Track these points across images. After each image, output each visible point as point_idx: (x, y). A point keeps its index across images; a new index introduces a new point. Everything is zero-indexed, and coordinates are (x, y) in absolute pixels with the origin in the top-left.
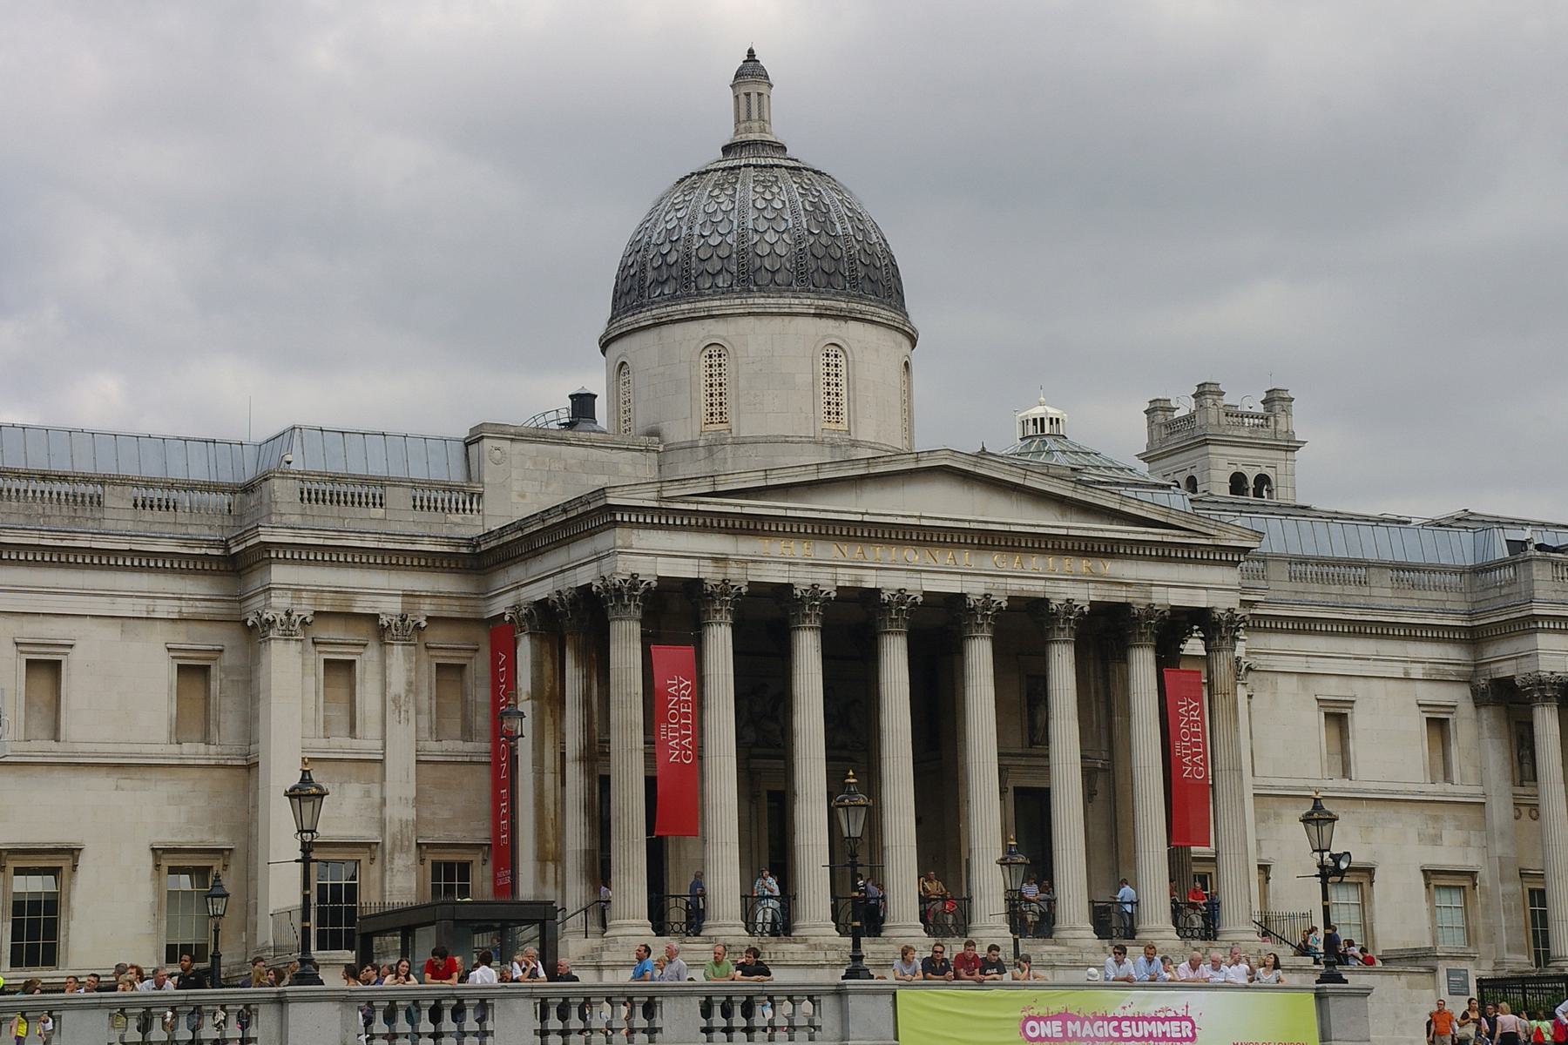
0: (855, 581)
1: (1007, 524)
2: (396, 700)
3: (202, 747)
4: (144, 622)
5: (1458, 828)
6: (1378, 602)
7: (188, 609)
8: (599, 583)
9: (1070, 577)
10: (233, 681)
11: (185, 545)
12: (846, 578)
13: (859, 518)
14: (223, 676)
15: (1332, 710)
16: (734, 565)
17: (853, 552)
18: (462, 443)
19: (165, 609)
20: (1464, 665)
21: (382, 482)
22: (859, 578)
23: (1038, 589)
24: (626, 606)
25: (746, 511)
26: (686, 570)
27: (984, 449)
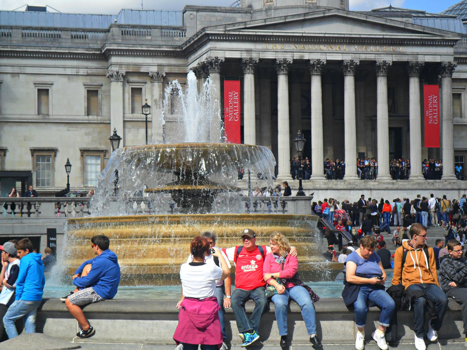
0: (301, 57)
1: (359, 35)
2: (155, 101)
3: (95, 117)
7: (90, 72)
8: (206, 60)
10: (106, 95)
12: (297, 56)
13: (301, 35)
14: (102, 93)
16: (254, 53)
17: (300, 47)
18: (182, 13)
19: (82, 72)
23: (372, 57)
24: (214, 68)
26: (236, 55)
27: (391, 6)
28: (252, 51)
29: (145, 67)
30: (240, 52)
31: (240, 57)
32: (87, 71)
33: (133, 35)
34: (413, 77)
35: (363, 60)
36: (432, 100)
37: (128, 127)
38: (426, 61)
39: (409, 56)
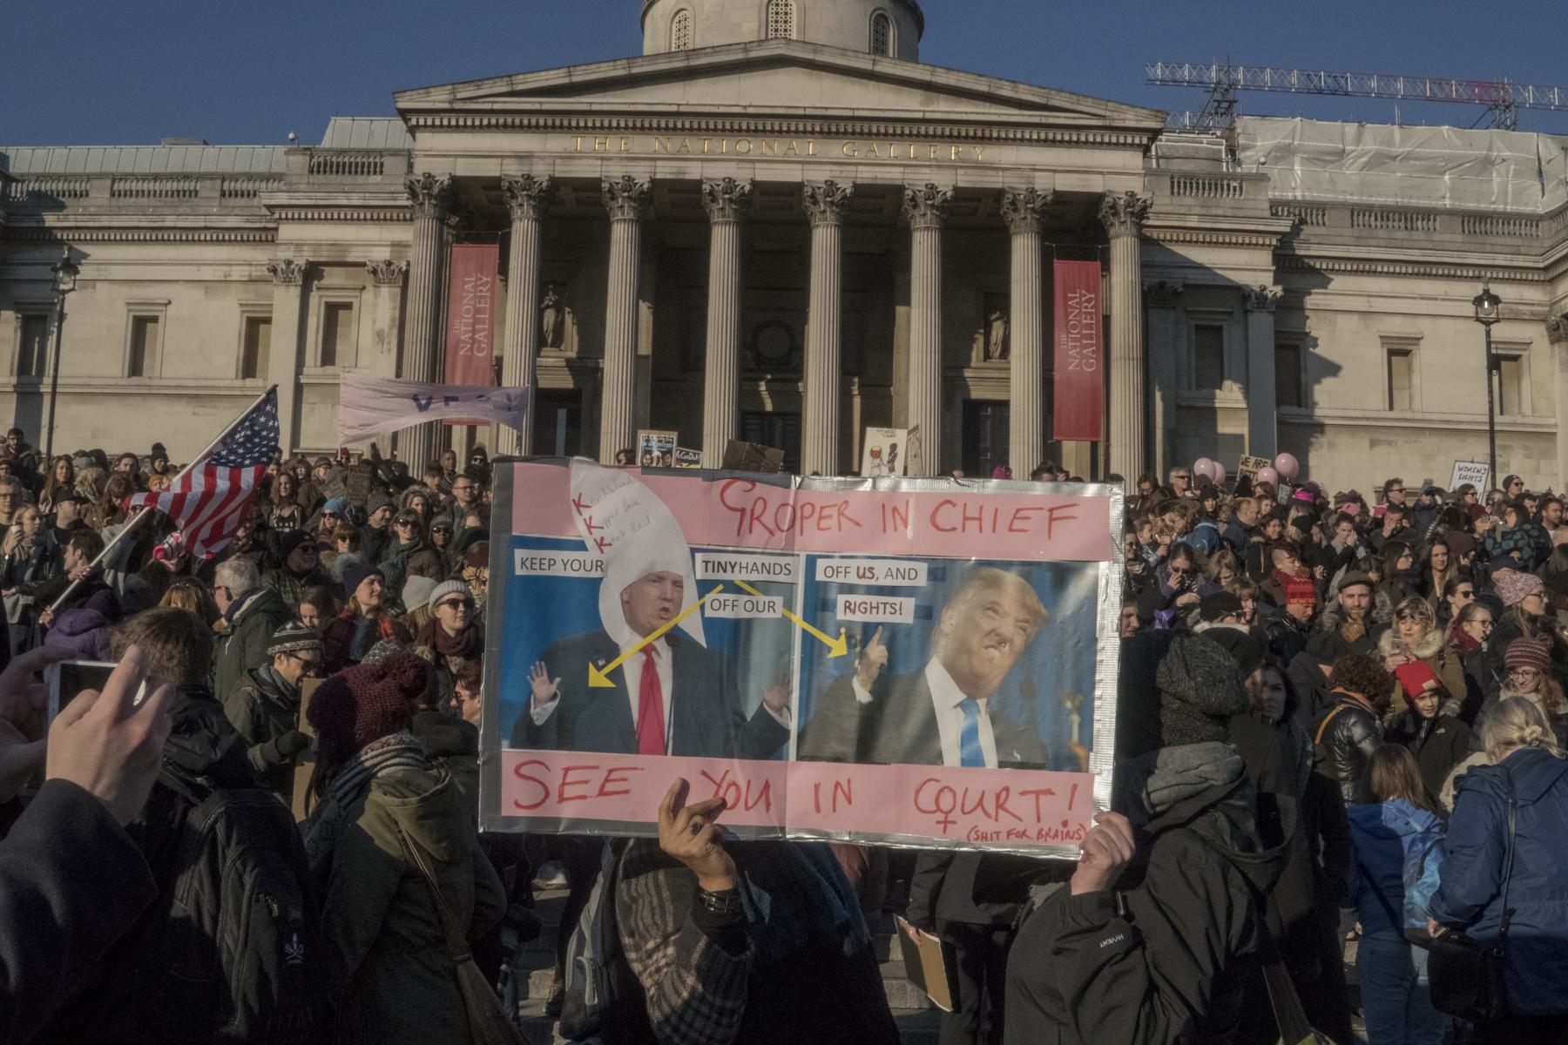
1: (851, 109)
4: (223, 284)
5: (1527, 457)
6: (1447, 246)
9: (934, 163)
11: (248, 221)
12: (665, 171)
13: (674, 109)
15: (1396, 347)
16: (541, 162)
20: (1539, 305)
21: (381, 153)
22: (682, 170)
23: (895, 176)
24: (422, 204)
25: (545, 107)
26: (489, 169)
28: (535, 157)
29: (359, 248)
30: (500, 160)
31: (497, 174)
32: (251, 271)
33: (337, 172)
34: (1017, 233)
35: (865, 182)
36: (1079, 303)
37: (311, 401)
38: (1059, 188)
39: (1007, 173)
